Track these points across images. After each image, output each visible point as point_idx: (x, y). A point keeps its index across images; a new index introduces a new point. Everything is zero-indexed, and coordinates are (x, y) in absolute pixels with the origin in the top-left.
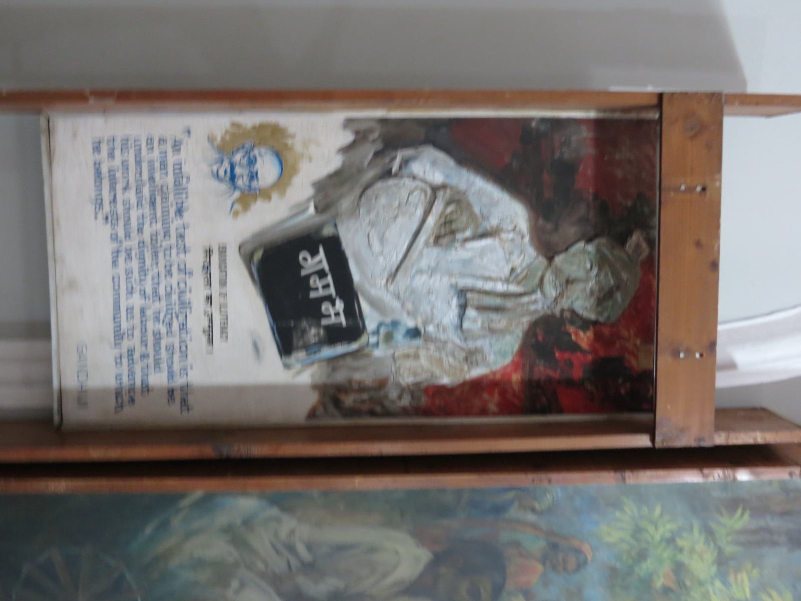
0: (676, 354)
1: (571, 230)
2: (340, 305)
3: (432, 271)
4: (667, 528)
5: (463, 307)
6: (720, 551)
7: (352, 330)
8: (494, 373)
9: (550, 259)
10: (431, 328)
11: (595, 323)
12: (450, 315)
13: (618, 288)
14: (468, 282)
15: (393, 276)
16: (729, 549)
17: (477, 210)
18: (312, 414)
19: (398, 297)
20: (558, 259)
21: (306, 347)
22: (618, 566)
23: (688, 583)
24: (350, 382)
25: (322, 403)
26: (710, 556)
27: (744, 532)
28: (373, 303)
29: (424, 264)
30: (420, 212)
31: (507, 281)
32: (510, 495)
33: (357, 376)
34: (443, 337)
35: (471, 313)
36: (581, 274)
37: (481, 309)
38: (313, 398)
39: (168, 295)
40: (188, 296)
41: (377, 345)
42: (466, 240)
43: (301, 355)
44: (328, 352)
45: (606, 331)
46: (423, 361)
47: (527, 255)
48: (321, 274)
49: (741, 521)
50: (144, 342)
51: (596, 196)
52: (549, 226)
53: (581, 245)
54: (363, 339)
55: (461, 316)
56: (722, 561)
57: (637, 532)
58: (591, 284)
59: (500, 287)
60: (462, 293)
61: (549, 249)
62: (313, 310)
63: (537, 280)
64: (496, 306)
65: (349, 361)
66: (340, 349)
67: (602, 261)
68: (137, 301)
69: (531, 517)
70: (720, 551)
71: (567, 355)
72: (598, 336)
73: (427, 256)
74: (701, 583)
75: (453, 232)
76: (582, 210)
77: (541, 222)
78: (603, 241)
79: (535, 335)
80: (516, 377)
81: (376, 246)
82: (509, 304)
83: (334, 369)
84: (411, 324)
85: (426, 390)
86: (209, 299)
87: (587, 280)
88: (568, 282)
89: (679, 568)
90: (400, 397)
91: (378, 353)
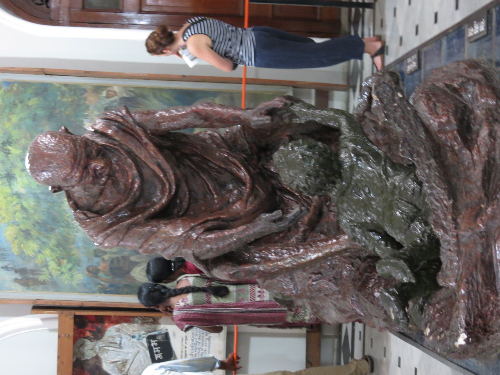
0: (69, 336)
1: (91, 363)
2: (152, 345)
3: (128, 353)
4: (64, 277)
5: (120, 344)
6: (48, 269)
7: (150, 338)
8: (112, 326)
9: (97, 355)
10: (129, 338)
11: (85, 338)
12: (124, 341)
13: (79, 347)
14: (119, 350)
15: (138, 352)
16: (44, 269)
17: (116, 368)
18: (160, 317)
19: (138, 347)
20: (95, 355)
21: (162, 334)
22: (78, 267)
23: (57, 260)
24: (151, 325)
25: (158, 319)
26: (50, 268)
27: (41, 274)
28: (143, 345)
29: (130, 355)
30: (131, 368)
31: (108, 350)
32: (108, 290)
33: (148, 326)
34: (126, 336)
35: (118, 342)
36: (89, 351)
37: (116, 343)
38: (160, 321)
39: (196, 349)
40: (191, 348)
41: (144, 334)
42: (119, 361)
43: (163, 332)
44: (156, 333)
45: (82, 336)
46: (131, 329)
47: (103, 356)
48: (157, 353)
49: (42, 278)
50: (203, 336)
51: (84, 371)
52: (97, 364)
53: (89, 359)
54: (146, 336)
55: (121, 341)
56: (47, 266)
57: (72, 277)
58: (86, 348)
59: (110, 348)
60: (121, 348)
61: (97, 358)
62: (159, 344)
63: (101, 349)
64: (112, 343)
65: (150, 330)
66: (153, 333)
67: (83, 354)
68: (204, 348)
69: (102, 283)
70: (48, 269)
71: (93, 329)
72: (84, 334)
73: (129, 357)
74: (53, 260)
75: (123, 363)
76: (88, 368)
77: (99, 365)
78: (83, 360)
79: (101, 335)
80: (106, 324)
81: (142, 359)
82: (108, 344)
83: (154, 328)
84: (134, 340)
85: (131, 322)
86: (186, 348)
87: (88, 349)
88: (92, 349)
89: (60, 265)
90: (138, 320)
91: (143, 332)
